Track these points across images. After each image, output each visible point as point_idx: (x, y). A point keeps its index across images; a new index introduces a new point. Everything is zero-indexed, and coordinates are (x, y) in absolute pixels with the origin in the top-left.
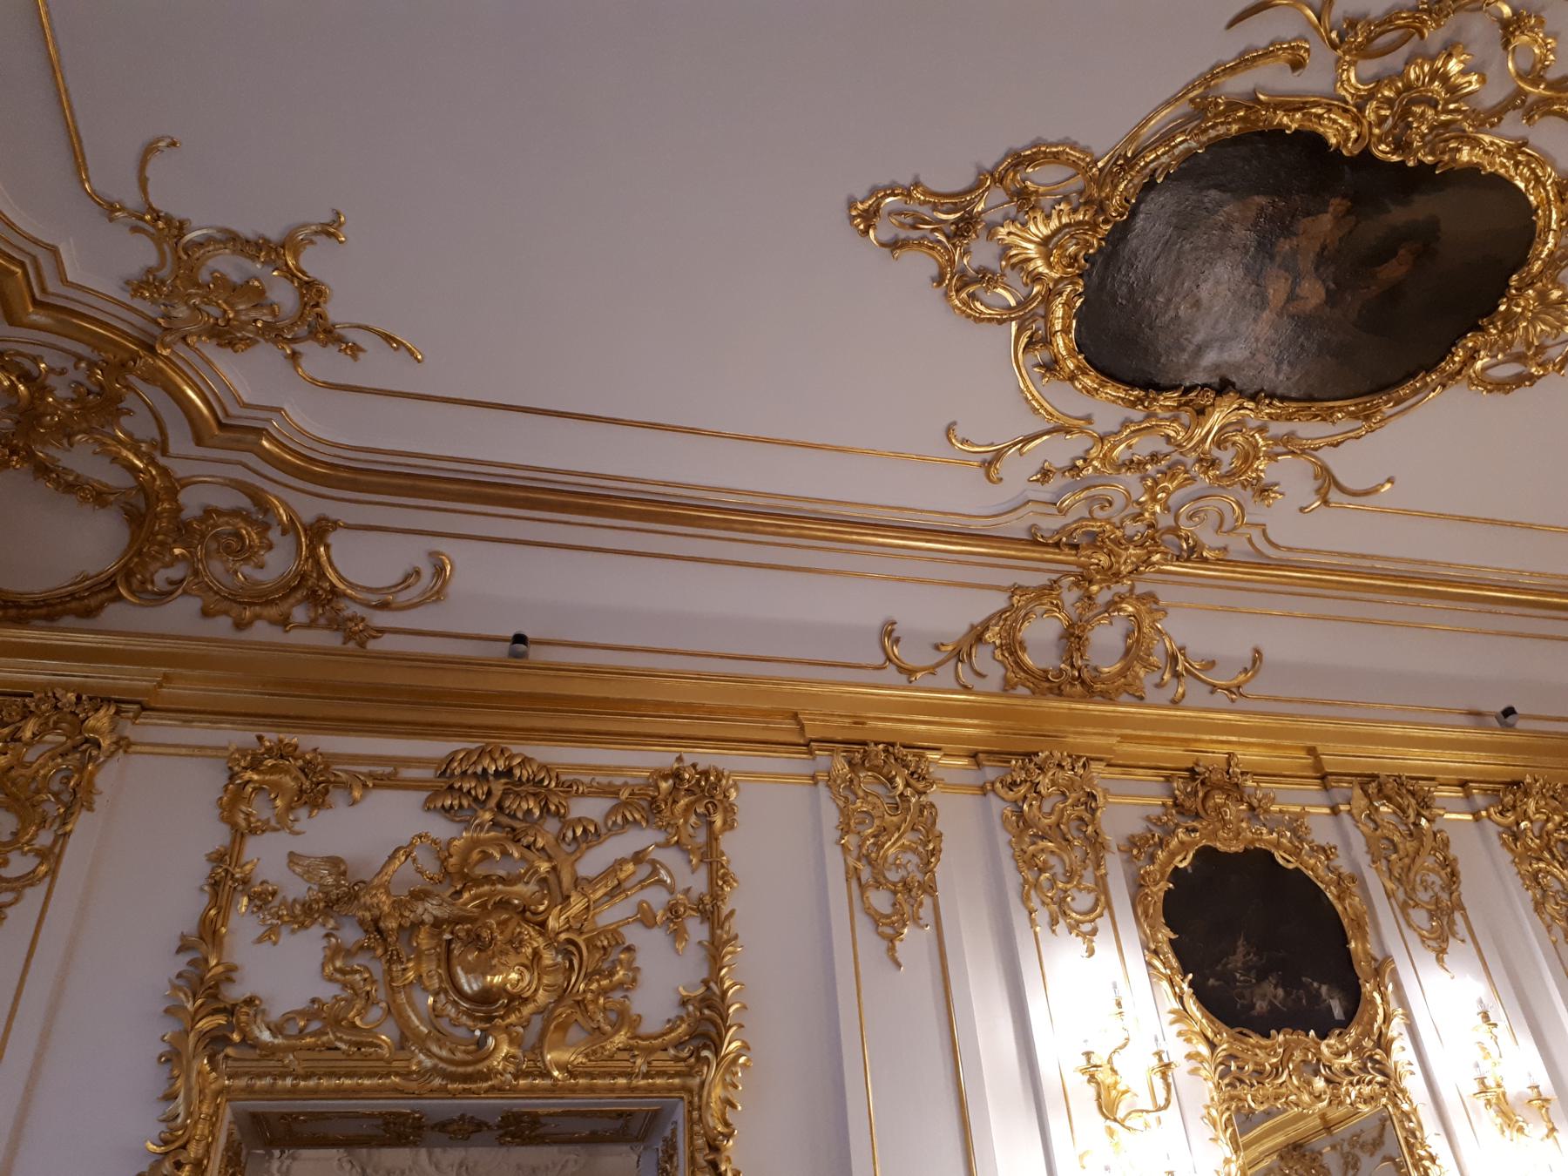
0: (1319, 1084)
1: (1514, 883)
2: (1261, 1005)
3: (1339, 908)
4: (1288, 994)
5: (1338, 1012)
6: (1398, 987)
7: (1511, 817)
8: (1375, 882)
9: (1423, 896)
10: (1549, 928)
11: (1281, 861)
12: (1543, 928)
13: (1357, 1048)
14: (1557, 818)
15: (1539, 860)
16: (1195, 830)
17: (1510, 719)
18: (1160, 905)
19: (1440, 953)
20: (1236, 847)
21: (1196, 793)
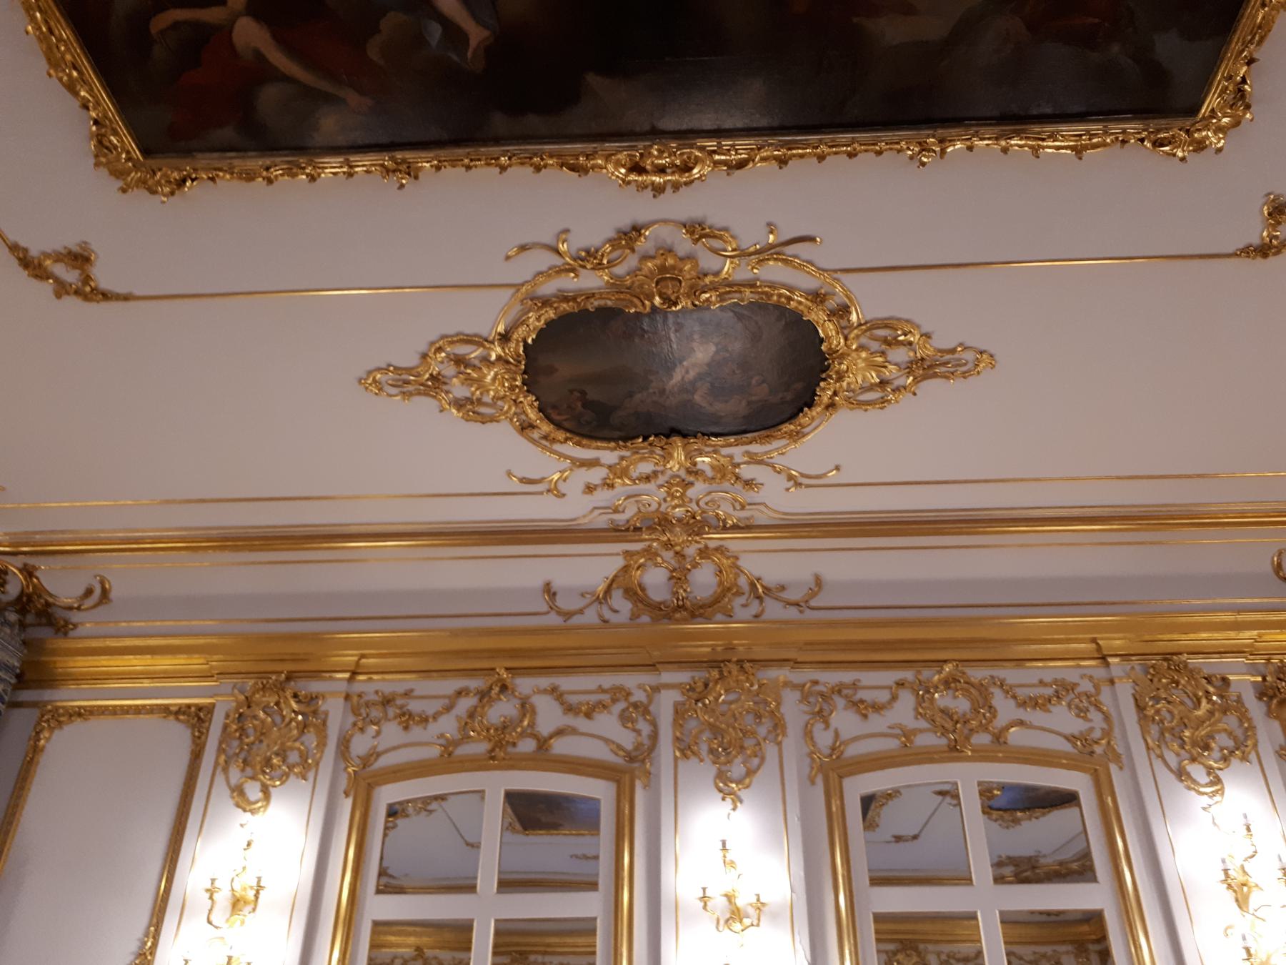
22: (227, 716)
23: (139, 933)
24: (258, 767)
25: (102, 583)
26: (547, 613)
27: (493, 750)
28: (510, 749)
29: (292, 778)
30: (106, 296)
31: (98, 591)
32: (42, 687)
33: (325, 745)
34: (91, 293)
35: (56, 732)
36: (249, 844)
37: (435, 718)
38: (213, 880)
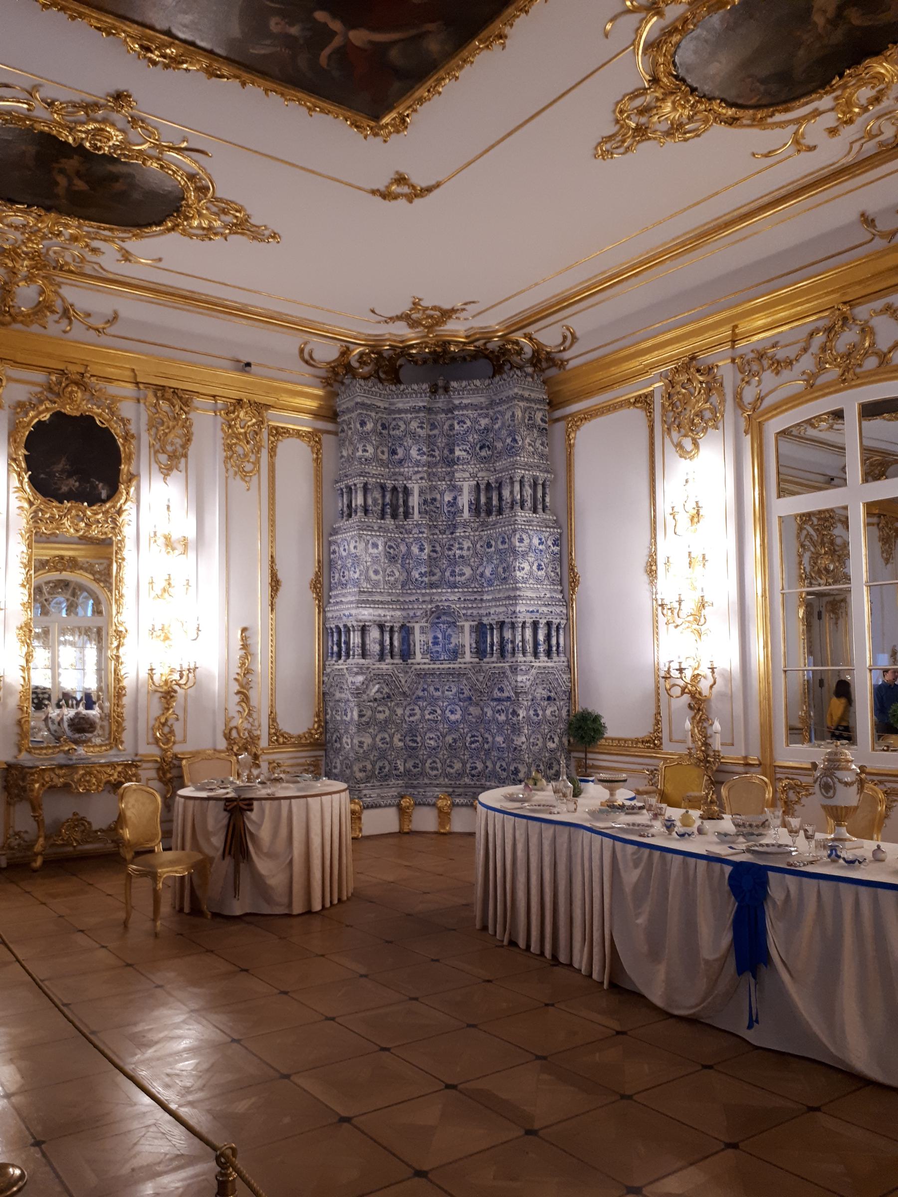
0: (82, 525)
1: (220, 447)
2: (65, 489)
3: (122, 449)
4: (80, 485)
5: (104, 495)
6: (138, 489)
7: (232, 416)
8: (145, 439)
9: (169, 448)
10: (227, 470)
11: (98, 422)
12: (225, 470)
13: (106, 513)
14: (254, 420)
15: (238, 439)
16: (55, 403)
17: (248, 369)
18: (25, 439)
19: (166, 475)
20: (78, 414)
21: (60, 383)
22: (663, 397)
23: (647, 544)
24: (687, 427)
25: (568, 329)
26: (872, 239)
27: (843, 375)
28: (858, 370)
29: (709, 430)
30: (429, 190)
31: (568, 334)
32: (564, 407)
33: (725, 401)
34: (418, 193)
35: (578, 432)
36: (687, 481)
37: (797, 360)
38: (673, 508)
